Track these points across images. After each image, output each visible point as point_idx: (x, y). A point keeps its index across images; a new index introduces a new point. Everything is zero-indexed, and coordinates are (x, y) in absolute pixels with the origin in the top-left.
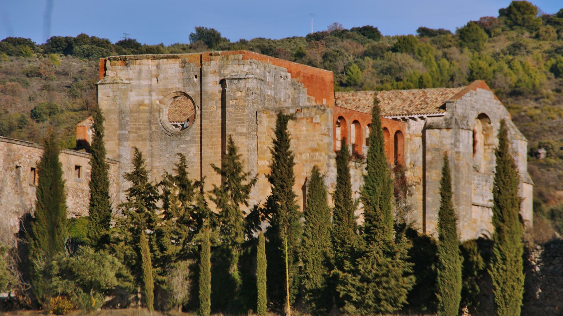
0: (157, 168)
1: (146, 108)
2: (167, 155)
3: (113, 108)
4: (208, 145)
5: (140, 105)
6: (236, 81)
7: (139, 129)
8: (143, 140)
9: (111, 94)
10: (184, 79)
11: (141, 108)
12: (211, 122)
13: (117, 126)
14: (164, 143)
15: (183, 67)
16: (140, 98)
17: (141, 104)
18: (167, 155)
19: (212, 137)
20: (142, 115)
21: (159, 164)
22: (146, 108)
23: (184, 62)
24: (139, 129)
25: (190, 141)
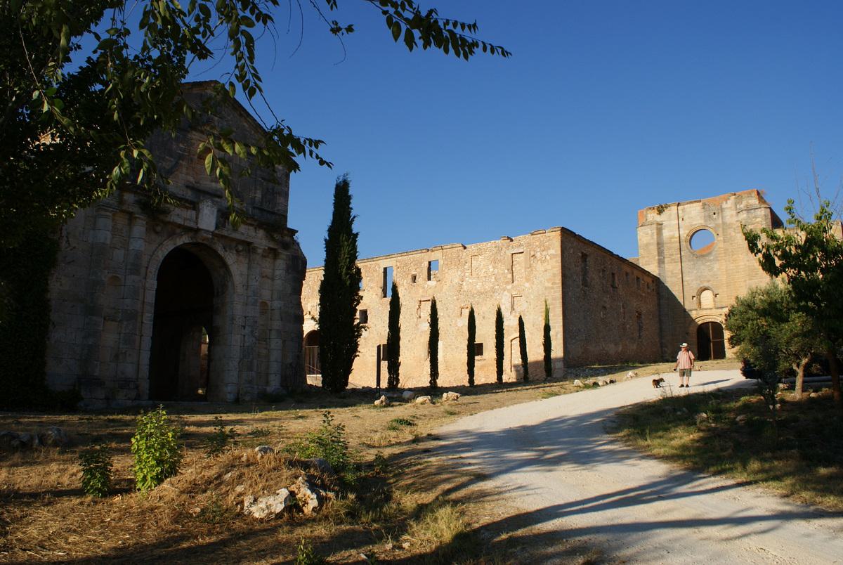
0: (687, 281)
1: (676, 240)
2: (695, 272)
3: (652, 241)
4: (729, 261)
5: (671, 238)
6: (753, 211)
7: (672, 255)
8: (675, 262)
9: (650, 232)
10: (705, 217)
11: (673, 240)
12: (731, 244)
13: (656, 253)
14: (692, 263)
15: (704, 208)
16: (672, 233)
17: (672, 237)
18: (695, 272)
19: (733, 255)
20: (674, 245)
21: (688, 278)
22: (676, 240)
23: (704, 204)
24: (672, 255)
25: (713, 260)
